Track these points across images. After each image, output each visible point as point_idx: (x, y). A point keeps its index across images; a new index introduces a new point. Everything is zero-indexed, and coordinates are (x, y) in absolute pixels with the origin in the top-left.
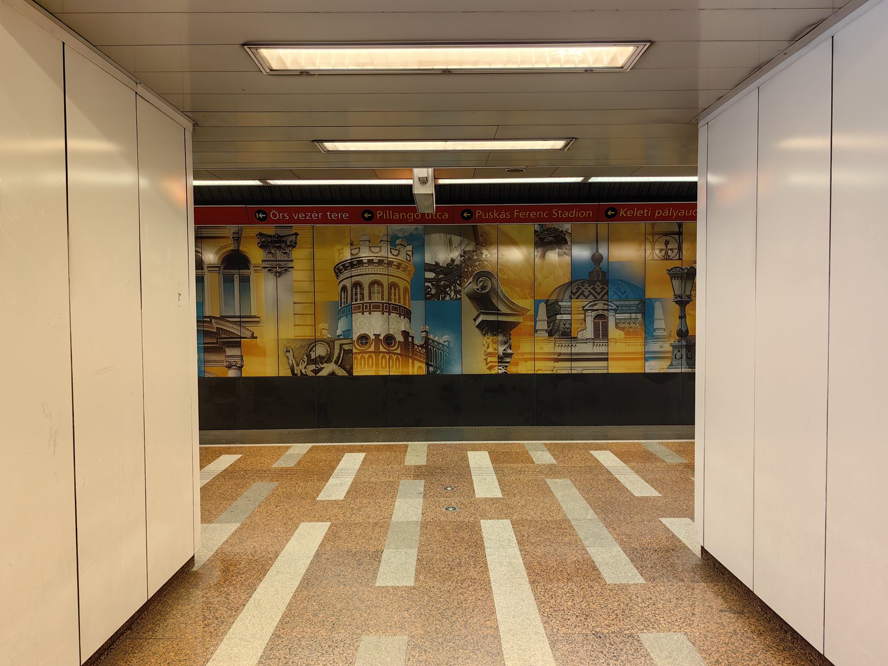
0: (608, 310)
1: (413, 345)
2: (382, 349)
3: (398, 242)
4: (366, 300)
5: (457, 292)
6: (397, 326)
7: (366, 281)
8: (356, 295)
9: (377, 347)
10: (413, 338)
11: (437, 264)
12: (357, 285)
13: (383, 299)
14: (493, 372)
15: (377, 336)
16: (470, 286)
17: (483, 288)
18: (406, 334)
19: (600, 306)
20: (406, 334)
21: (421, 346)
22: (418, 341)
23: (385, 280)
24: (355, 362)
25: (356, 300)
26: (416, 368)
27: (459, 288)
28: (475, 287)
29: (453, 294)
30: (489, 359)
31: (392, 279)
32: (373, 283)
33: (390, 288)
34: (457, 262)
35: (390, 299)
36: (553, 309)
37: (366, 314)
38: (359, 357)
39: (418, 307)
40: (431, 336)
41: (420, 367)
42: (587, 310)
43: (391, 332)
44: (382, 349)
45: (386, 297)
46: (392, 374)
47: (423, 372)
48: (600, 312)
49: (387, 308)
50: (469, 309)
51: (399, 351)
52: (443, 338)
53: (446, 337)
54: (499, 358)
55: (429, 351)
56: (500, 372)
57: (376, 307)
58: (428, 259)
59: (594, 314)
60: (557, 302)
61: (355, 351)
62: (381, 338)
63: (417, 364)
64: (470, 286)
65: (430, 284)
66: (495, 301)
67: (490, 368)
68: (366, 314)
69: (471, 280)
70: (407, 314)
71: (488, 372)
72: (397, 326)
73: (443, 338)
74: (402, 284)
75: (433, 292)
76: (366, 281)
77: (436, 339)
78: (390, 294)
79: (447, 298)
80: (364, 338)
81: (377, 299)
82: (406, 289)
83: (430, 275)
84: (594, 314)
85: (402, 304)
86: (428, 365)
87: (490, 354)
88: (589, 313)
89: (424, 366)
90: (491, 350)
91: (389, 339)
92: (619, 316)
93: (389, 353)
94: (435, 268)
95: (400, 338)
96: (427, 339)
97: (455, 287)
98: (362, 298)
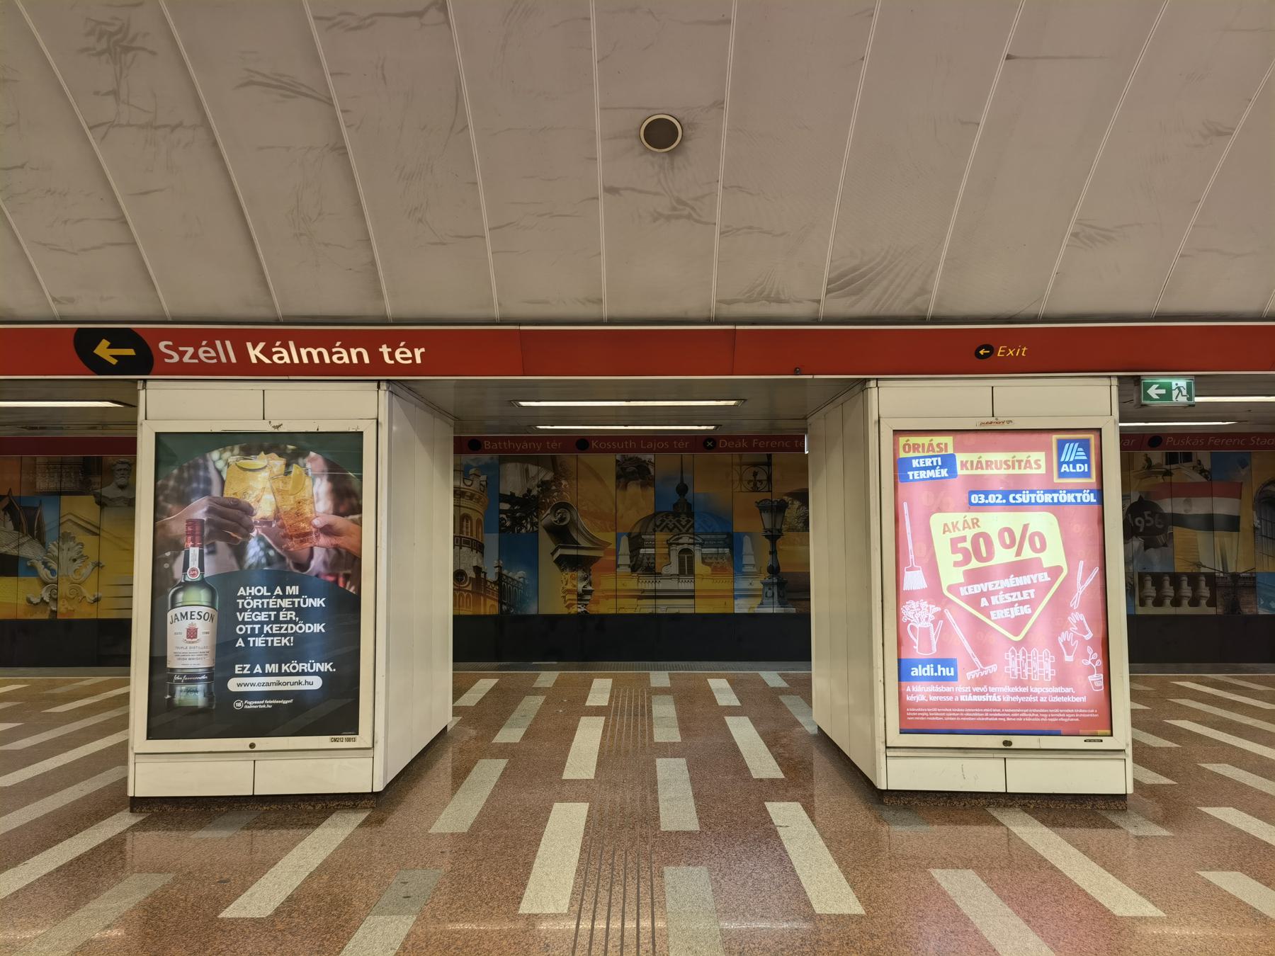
0: (694, 544)
19: (685, 539)
36: (636, 543)
42: (671, 544)
48: (686, 546)
52: (519, 574)
59: (679, 548)
60: (639, 535)
73: (519, 574)
84: (679, 548)
88: (673, 547)
92: (705, 551)
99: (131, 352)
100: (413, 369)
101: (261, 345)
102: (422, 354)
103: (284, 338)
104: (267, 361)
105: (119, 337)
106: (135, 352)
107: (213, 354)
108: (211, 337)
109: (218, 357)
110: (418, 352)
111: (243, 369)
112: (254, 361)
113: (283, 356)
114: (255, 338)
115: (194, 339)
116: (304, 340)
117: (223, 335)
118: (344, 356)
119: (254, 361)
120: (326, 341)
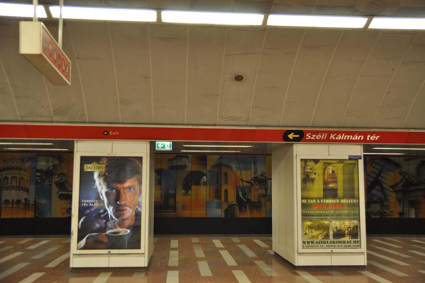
1: (29, 203)
2: (15, 206)
3: (25, 160)
4: (9, 184)
5: (50, 181)
6: (22, 196)
7: (10, 176)
8: (5, 182)
9: (12, 205)
10: (29, 201)
11: (42, 169)
12: (6, 178)
13: (17, 184)
14: (65, 216)
15: (13, 200)
16: (56, 179)
17: (62, 180)
18: (26, 199)
20: (26, 199)
21: (33, 205)
22: (32, 202)
23: (17, 176)
24: (2, 211)
25: (5, 184)
26: (30, 214)
27: (51, 179)
28: (58, 179)
29: (48, 182)
30: (63, 210)
31: (21, 176)
32: (13, 178)
33: (20, 179)
34: (51, 169)
35: (20, 184)
37: (9, 191)
38: (4, 209)
39: (32, 188)
40: (37, 200)
41: (32, 214)
43: (20, 198)
44: (15, 206)
45: (18, 183)
46: (19, 217)
47: (32, 216)
49: (19, 188)
50: (55, 190)
51: (22, 207)
53: (44, 201)
54: (67, 210)
55: (36, 207)
56: (67, 216)
57: (14, 188)
58: (39, 168)
61: (2, 207)
62: (15, 201)
63: (30, 213)
64: (56, 179)
65: (38, 178)
66: (66, 185)
67: (63, 214)
68: (9, 191)
69: (56, 176)
70: (27, 191)
71: (62, 216)
72: (22, 196)
74: (26, 178)
75: (40, 181)
76: (10, 176)
77: (40, 201)
78: (20, 182)
79: (46, 184)
80: (7, 201)
81: (14, 184)
82: (27, 180)
83: (39, 174)
85: (25, 186)
86: (35, 213)
87: (63, 208)
89: (33, 213)
90: (64, 206)
91: (18, 202)
93: (18, 208)
94: (41, 171)
95: (23, 201)
96: (35, 202)
97: (49, 179)
98: (8, 184)
99: (298, 136)
100: (375, 141)
101: (335, 135)
102: (378, 138)
103: (341, 133)
104: (334, 138)
105: (296, 132)
106: (301, 137)
107: (320, 137)
108: (322, 132)
109: (321, 138)
110: (377, 137)
111: (328, 141)
112: (331, 138)
113: (339, 137)
114: (333, 132)
115: (316, 133)
116: (347, 133)
117: (325, 132)
118: (356, 138)
119: (331, 138)
120: (353, 134)
